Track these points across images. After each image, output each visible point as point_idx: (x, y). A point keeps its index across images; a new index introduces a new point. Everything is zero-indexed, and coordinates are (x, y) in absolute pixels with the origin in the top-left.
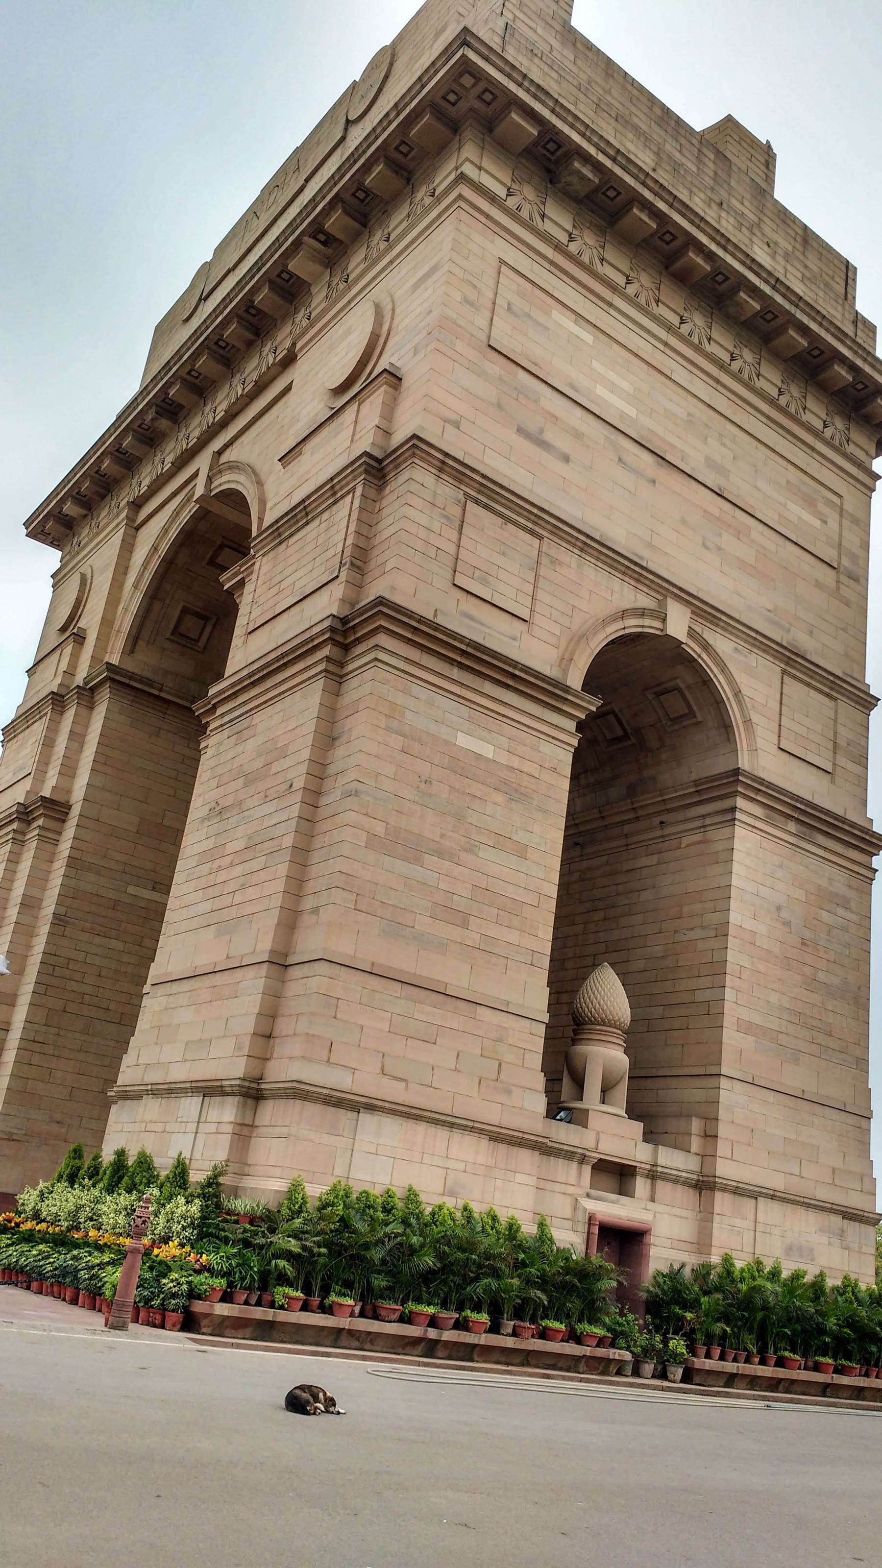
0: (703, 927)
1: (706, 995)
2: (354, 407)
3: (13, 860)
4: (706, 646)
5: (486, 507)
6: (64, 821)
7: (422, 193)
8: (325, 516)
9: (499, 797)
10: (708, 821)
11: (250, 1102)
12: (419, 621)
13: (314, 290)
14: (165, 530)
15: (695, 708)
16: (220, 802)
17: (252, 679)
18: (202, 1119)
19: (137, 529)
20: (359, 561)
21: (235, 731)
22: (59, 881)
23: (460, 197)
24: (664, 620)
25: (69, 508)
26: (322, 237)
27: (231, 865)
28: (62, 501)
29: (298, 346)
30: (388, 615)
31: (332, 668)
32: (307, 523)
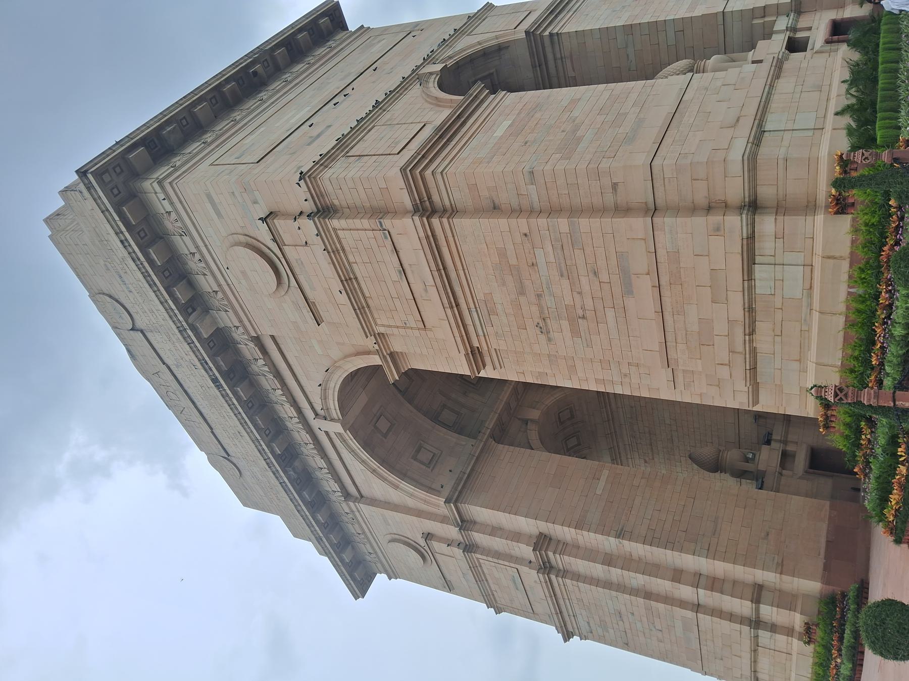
0: (627, 47)
1: (671, 34)
2: (286, 249)
3: (578, 577)
4: (450, 58)
5: (352, 148)
6: (550, 539)
8: (351, 259)
9: (538, 115)
10: (558, 56)
11: (759, 211)
12: (419, 154)
14: (363, 462)
15: (487, 73)
16: (537, 320)
17: (454, 304)
18: (772, 260)
19: (362, 496)
20: (380, 212)
21: (488, 318)
22: (592, 534)
23: (170, 183)
24: (431, 74)
25: (347, 556)
26: (190, 310)
27: (580, 293)
28: (342, 560)
30: (413, 172)
31: (447, 215)
32: (356, 278)
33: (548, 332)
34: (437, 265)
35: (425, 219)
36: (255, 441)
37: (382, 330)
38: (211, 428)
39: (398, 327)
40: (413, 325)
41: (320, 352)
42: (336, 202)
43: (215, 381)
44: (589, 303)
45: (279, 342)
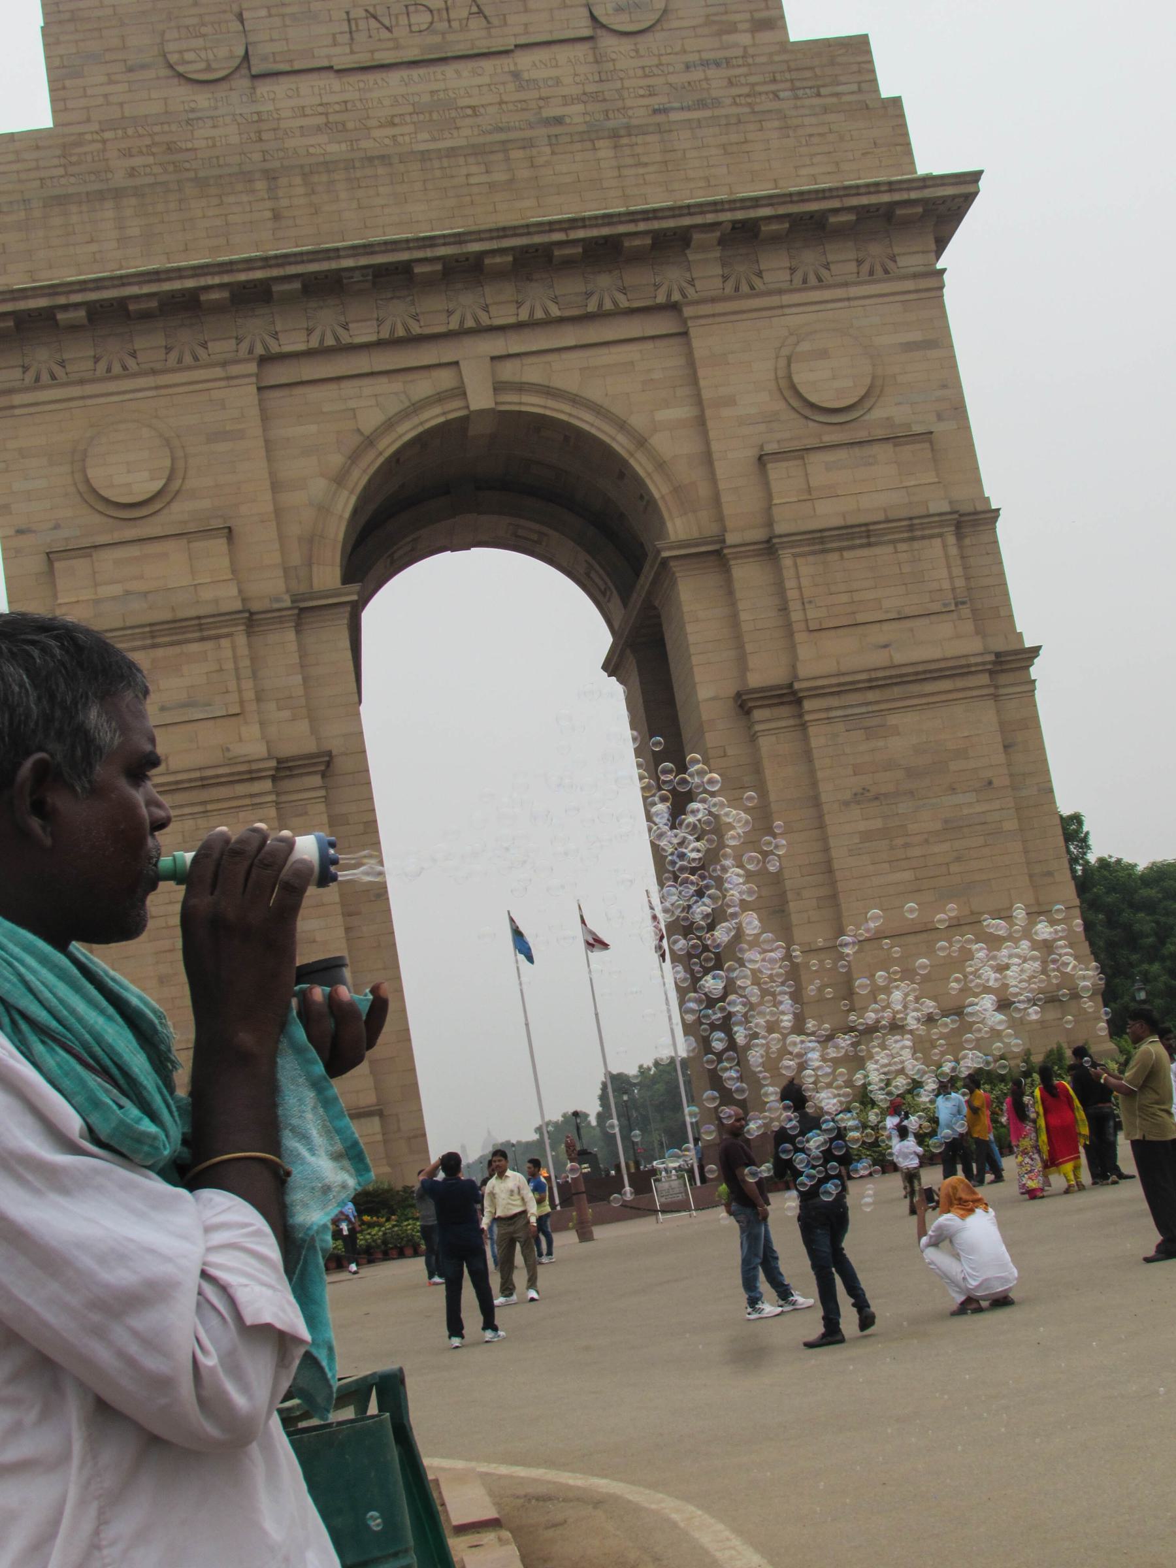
7: (876, 249)
8: (902, 547)
13: (692, 256)
14: (389, 425)
17: (874, 684)
27: (927, 841)
28: (65, 308)
29: (688, 311)
32: (869, 545)
33: (858, 803)
34: (930, 671)
35: (989, 667)
36: (459, 239)
37: (787, 562)
38: (339, 71)
39: (800, 588)
40: (811, 614)
41: (664, 415)
42: (967, 541)
43: (608, 219)
44: (916, 852)
45: (658, 343)
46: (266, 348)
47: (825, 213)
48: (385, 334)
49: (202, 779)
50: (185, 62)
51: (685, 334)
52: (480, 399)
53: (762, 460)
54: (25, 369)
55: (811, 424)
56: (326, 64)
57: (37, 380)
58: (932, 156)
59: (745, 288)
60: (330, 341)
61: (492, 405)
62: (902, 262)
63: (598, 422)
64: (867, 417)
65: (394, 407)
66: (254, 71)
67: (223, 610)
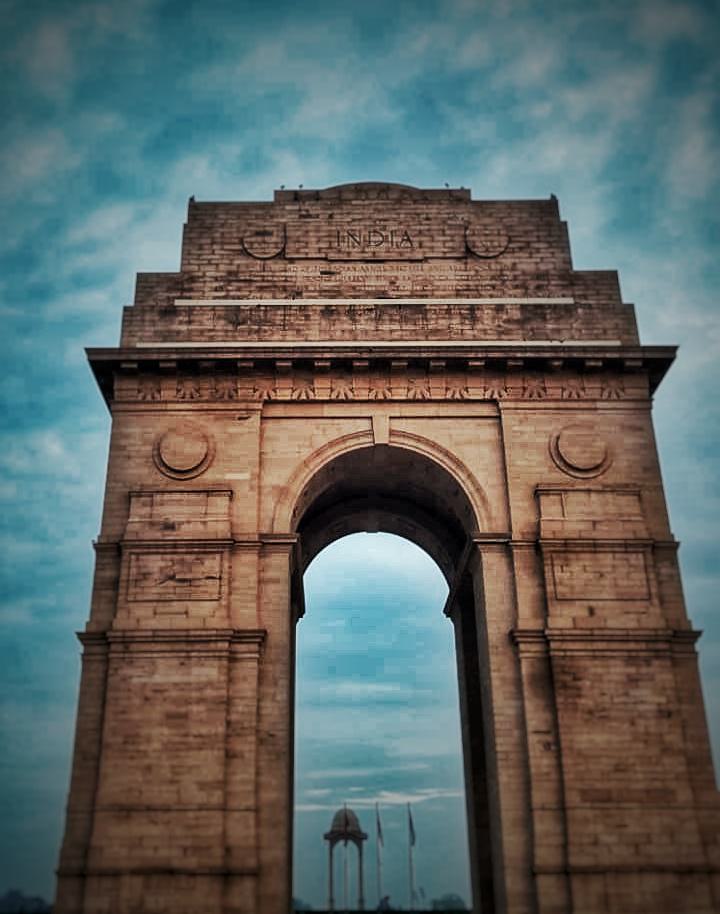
29: (501, 405)
46: (269, 395)
47: (583, 360)
48: (333, 397)
49: (187, 636)
50: (252, 248)
51: (499, 417)
52: (382, 438)
53: (537, 493)
54: (139, 391)
55: (567, 476)
56: (323, 256)
57: (144, 397)
58: (649, 336)
59: (535, 396)
60: (304, 397)
61: (386, 442)
62: (629, 391)
63: (446, 460)
64: (601, 477)
65: (334, 435)
66: (288, 256)
67: (220, 537)
